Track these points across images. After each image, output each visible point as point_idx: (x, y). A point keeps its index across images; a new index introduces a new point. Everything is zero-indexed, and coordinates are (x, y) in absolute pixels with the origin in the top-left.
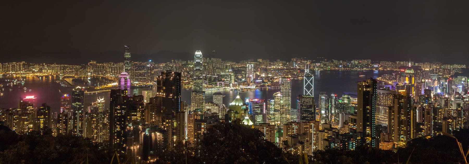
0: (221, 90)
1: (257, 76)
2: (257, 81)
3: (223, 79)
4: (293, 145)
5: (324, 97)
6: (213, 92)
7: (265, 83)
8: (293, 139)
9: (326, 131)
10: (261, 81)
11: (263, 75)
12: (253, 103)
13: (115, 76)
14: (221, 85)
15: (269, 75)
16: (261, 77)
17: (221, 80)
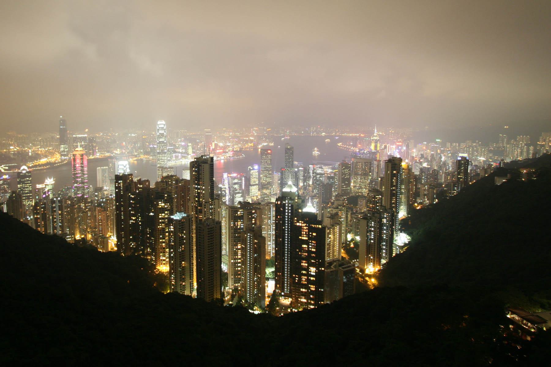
0: (179, 163)
1: (216, 145)
2: (218, 151)
3: (177, 150)
4: (332, 226)
5: (302, 169)
6: (170, 165)
7: (226, 153)
8: (331, 220)
9: (339, 207)
10: (222, 151)
11: (221, 144)
12: (231, 179)
13: (45, 150)
14: (177, 157)
15: (227, 144)
16: (220, 146)
17: (175, 152)
